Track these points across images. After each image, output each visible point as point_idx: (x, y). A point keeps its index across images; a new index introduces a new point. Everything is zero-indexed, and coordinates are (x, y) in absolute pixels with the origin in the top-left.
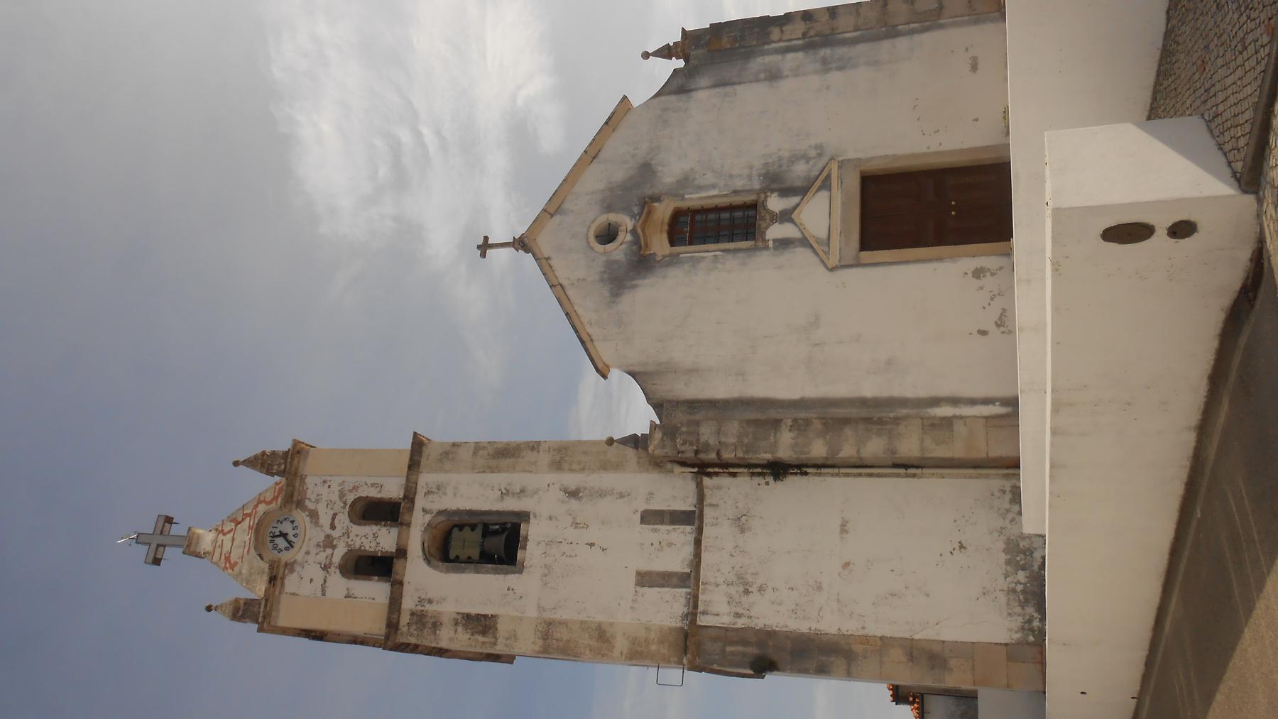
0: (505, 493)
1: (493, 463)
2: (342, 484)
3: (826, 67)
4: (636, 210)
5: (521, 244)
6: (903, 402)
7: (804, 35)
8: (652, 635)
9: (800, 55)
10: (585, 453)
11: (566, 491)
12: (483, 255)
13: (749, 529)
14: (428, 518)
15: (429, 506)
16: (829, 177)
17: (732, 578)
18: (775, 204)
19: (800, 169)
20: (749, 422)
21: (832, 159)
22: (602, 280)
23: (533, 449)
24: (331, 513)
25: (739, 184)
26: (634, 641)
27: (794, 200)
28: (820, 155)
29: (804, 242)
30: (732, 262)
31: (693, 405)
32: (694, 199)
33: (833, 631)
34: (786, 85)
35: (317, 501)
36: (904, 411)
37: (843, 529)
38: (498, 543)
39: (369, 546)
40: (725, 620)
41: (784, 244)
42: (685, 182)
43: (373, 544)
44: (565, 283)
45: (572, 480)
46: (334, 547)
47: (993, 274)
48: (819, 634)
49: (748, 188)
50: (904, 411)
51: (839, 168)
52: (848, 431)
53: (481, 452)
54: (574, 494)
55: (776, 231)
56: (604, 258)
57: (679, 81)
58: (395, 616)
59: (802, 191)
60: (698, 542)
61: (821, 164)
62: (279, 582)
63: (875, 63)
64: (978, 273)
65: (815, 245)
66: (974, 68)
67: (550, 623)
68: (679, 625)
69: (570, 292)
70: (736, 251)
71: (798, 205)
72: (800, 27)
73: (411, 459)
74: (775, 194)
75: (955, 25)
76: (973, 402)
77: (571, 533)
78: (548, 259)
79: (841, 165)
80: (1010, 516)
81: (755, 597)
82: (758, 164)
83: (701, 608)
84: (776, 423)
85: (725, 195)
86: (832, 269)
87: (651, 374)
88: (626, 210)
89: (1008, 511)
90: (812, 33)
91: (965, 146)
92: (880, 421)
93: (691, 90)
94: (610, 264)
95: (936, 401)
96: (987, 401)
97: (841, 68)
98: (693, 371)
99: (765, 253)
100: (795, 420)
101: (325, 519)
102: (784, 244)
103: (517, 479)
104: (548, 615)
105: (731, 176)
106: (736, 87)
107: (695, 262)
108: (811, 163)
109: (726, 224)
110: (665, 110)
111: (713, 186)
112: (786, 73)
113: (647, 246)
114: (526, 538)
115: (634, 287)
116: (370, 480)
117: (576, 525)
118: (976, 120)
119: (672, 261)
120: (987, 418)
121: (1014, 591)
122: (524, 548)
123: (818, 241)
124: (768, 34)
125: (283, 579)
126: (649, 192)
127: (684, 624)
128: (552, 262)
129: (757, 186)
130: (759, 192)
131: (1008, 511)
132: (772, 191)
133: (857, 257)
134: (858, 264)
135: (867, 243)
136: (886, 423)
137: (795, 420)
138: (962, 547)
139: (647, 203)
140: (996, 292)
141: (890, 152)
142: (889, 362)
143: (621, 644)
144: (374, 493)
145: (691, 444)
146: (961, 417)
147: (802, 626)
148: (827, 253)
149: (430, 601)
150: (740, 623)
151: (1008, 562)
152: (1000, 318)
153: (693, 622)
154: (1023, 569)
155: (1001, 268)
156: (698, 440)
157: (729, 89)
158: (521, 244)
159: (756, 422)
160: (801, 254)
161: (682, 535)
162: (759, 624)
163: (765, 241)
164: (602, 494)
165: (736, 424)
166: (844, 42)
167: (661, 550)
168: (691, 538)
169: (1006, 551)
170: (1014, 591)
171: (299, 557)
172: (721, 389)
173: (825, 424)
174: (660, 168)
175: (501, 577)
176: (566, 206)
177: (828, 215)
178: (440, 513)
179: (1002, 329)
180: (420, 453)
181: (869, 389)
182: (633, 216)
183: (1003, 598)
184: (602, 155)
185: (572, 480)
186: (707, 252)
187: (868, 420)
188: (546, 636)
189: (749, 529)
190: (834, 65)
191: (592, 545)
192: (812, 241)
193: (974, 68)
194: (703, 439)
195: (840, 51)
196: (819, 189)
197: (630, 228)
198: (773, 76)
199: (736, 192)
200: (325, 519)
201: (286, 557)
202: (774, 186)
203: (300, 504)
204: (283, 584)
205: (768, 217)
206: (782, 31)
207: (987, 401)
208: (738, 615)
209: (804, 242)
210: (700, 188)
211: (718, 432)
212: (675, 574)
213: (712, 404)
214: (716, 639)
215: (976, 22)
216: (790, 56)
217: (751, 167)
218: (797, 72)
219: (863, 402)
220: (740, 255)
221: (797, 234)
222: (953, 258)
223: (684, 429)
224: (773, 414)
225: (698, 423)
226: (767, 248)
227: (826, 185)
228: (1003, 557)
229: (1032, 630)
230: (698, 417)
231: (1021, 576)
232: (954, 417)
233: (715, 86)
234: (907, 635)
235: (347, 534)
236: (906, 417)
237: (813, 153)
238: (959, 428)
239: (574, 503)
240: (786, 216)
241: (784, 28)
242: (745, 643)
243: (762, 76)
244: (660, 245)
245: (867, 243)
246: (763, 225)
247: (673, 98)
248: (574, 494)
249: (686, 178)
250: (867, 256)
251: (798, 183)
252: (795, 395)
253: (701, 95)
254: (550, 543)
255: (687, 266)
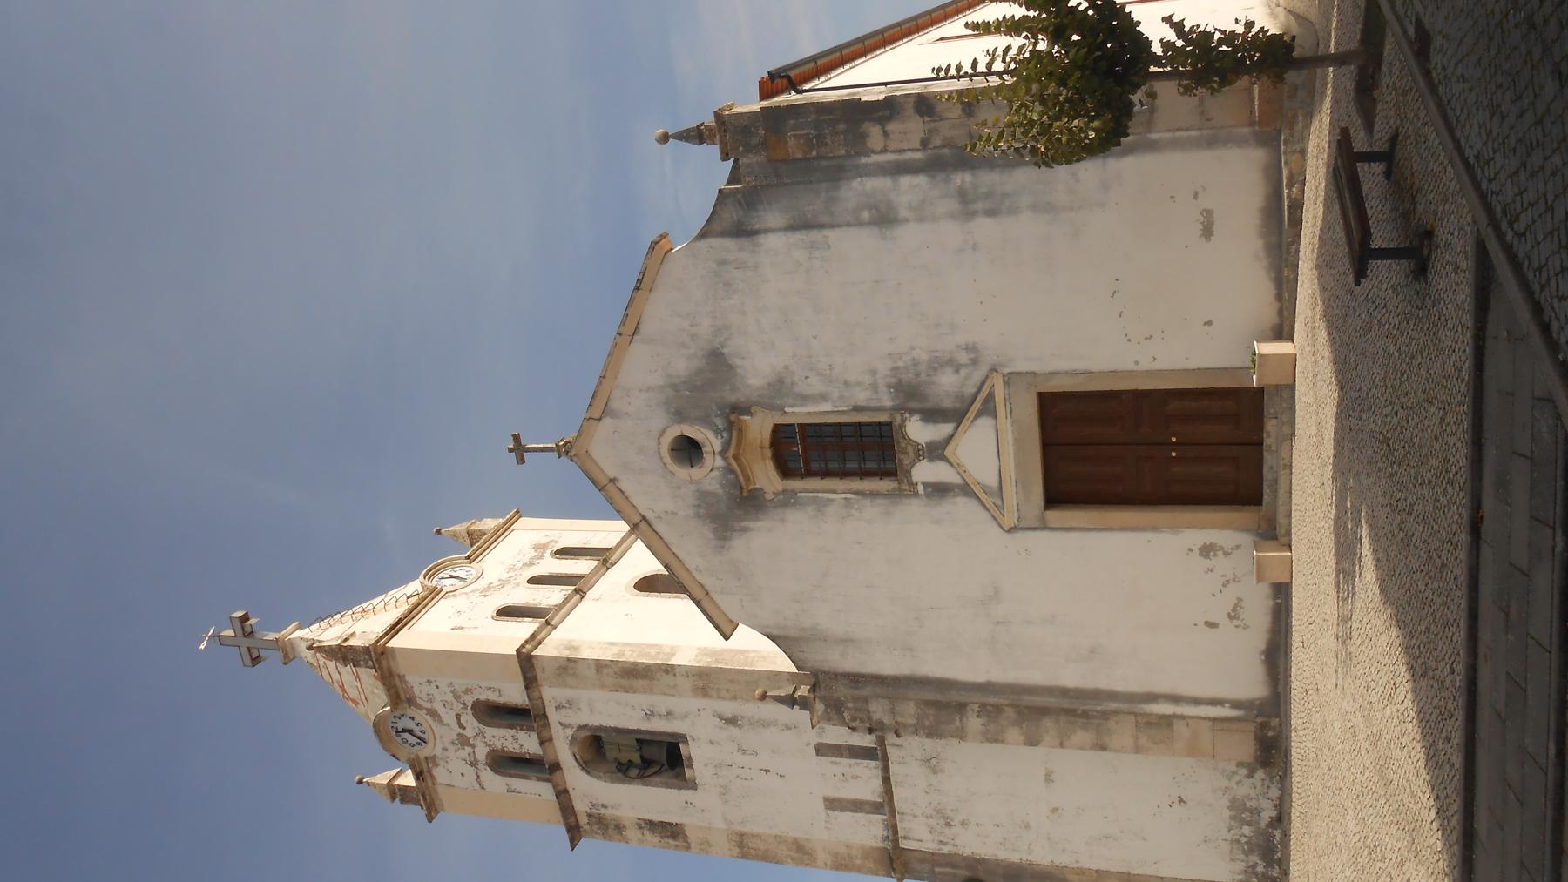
0: (650, 715)
1: (625, 682)
2: (451, 684)
3: (967, 208)
4: (720, 423)
5: (565, 450)
6: (1113, 696)
7: (924, 144)
8: (854, 852)
9: (921, 180)
10: (732, 681)
11: (721, 718)
12: (521, 460)
13: (942, 771)
14: (570, 732)
15: (563, 721)
16: (990, 397)
17: (929, 812)
18: (918, 431)
19: (947, 384)
20: (928, 703)
21: (993, 370)
22: (698, 516)
23: (667, 672)
24: (453, 714)
25: (862, 397)
26: (836, 855)
27: (945, 429)
28: (974, 362)
29: (966, 490)
30: (871, 510)
31: (856, 679)
32: (799, 413)
33: (1046, 862)
34: (909, 235)
35: (431, 701)
36: (1113, 706)
37: (1048, 778)
38: (662, 755)
39: (512, 747)
40: (929, 845)
41: (939, 490)
42: (780, 387)
43: (516, 746)
44: (649, 515)
45: (729, 708)
46: (473, 746)
47: (1226, 554)
48: (1030, 864)
49: (873, 404)
50: (1113, 706)
51: (1006, 384)
52: (1048, 722)
53: (605, 671)
54: (732, 721)
55: (924, 472)
56: (693, 488)
57: (731, 215)
58: (572, 820)
59: (956, 415)
60: (886, 780)
61: (978, 376)
62: (426, 775)
63: (1045, 208)
64: (1207, 551)
65: (983, 496)
66: (1207, 232)
67: (742, 835)
68: (881, 845)
69: (659, 528)
70: (874, 495)
71: (951, 437)
72: (911, 129)
73: (525, 678)
74: (916, 417)
75: (1176, 145)
76: (1197, 701)
77: (740, 759)
78: (612, 481)
79: (1009, 380)
80: (1237, 778)
81: (957, 829)
82: (884, 368)
83: (901, 833)
84: (961, 707)
85: (842, 412)
86: (1011, 530)
87: (796, 640)
88: (705, 421)
89: (1234, 773)
90: (937, 141)
91: (1192, 364)
92: (1085, 715)
93: (756, 233)
94: (703, 496)
95: (1153, 698)
96: (1214, 702)
97: (992, 213)
98: (847, 641)
99: (915, 501)
100: (983, 706)
101: (449, 718)
102: (939, 490)
103: (662, 703)
104: (738, 828)
105: (846, 383)
106: (827, 232)
107: (822, 505)
108: (963, 372)
109: (851, 452)
110: (722, 263)
111: (824, 397)
112: (903, 213)
113: (748, 479)
114: (690, 758)
115: (745, 530)
116: (484, 684)
117: (744, 752)
118: (1209, 323)
119: (788, 500)
120: (1214, 720)
121: (1238, 842)
122: (691, 767)
123: (985, 489)
124: (863, 137)
125: (430, 771)
126: (732, 398)
127: (888, 845)
128: (623, 486)
129: (888, 403)
130: (895, 409)
131: (1234, 773)
132: (912, 412)
133: (1043, 519)
134: (1044, 527)
135: (1054, 499)
136: (1093, 717)
137: (983, 706)
138: (1181, 800)
139: (733, 416)
140: (1230, 577)
141: (1080, 365)
142: (1092, 651)
143: (822, 857)
144: (493, 697)
145: (862, 721)
146: (1183, 717)
147: (1014, 857)
148: (1000, 508)
149: (603, 806)
150: (946, 850)
151: (1233, 818)
152: (1234, 610)
153: (896, 841)
154: (1249, 824)
155: (1238, 547)
156: (870, 718)
157: (815, 235)
158: (565, 450)
159: (935, 704)
160: (962, 506)
161: (868, 772)
162: (967, 852)
163: (912, 485)
164: (764, 724)
165: (912, 704)
166: (988, 163)
167: (846, 780)
168: (879, 773)
169: (1230, 808)
170: (1238, 842)
171: (438, 751)
172: (888, 665)
173: (1019, 713)
174: (737, 361)
175: (674, 791)
176: (616, 404)
177: (995, 451)
178: (581, 728)
179: (1236, 622)
180: (532, 667)
181: (1070, 678)
182: (717, 432)
183: (1226, 847)
184: (644, 328)
185: (729, 708)
186: (836, 491)
187: (1071, 712)
188: (741, 845)
189: (942, 771)
190: (979, 206)
191: (767, 771)
192: (977, 489)
193: (1207, 232)
194: (875, 717)
195: (988, 179)
196: (979, 415)
197: (718, 448)
198: (885, 218)
199: (858, 409)
200: (449, 718)
201: (424, 752)
202: (913, 405)
203: (411, 701)
204: (432, 777)
205: (910, 449)
206: (886, 134)
207: (1214, 702)
208: (941, 842)
209: (966, 490)
210: (805, 399)
211: (893, 712)
212: (867, 802)
213: (879, 680)
214: (923, 861)
215: (1211, 143)
216: (906, 181)
217: (874, 373)
218: (921, 214)
219: (1064, 692)
220: (880, 501)
221: (957, 480)
222: (1174, 528)
223: (850, 705)
224: (955, 697)
225: (866, 700)
226: (916, 494)
227: (988, 409)
228: (1227, 813)
229: (1256, 874)
230: (865, 692)
231: (1246, 830)
232: (1175, 716)
233: (792, 228)
234: (1124, 870)
235: (481, 734)
236: (1116, 712)
237: (963, 358)
238: (1179, 726)
239: (733, 729)
240: (935, 451)
241: (890, 127)
242: (953, 866)
243: (866, 215)
244: (766, 477)
245: (1054, 499)
246: (906, 462)
247: (729, 243)
248: (732, 721)
249: (781, 381)
250: (1054, 516)
251: (947, 403)
252: (981, 678)
253: (773, 241)
254: (719, 765)
255: (810, 509)
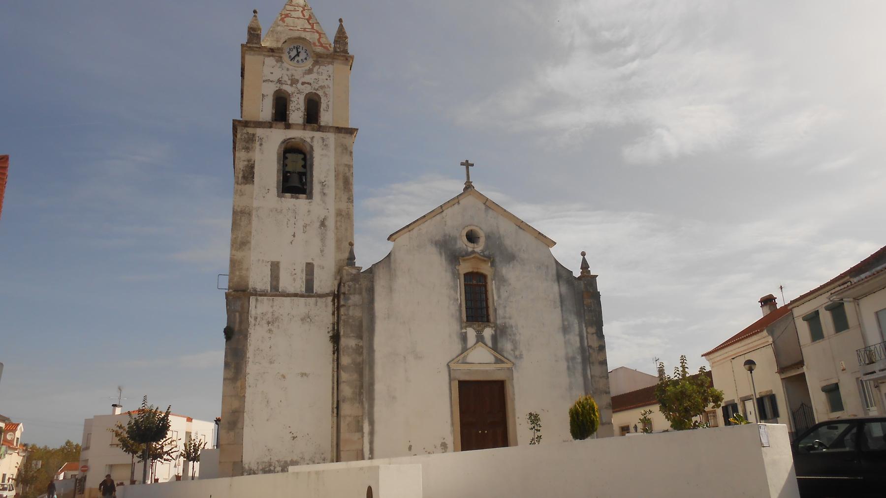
0: (323, 184)
1: (341, 176)
2: (329, 87)
3: (570, 359)
4: (486, 253)
6: (371, 406)
7: (590, 347)
8: (244, 272)
9: (578, 344)
10: (346, 230)
12: (462, 164)
14: (309, 140)
15: (315, 140)
16: (503, 362)
17: (276, 315)
18: (488, 333)
19: (507, 346)
21: (514, 364)
22: (445, 236)
23: (349, 199)
24: (311, 82)
25: (500, 312)
27: (490, 344)
28: (516, 357)
29: (465, 349)
30: (454, 309)
31: (371, 291)
32: (492, 286)
33: (248, 370)
34: (560, 337)
35: (318, 73)
36: (366, 406)
37: (303, 375)
39: (292, 106)
40: (253, 312)
41: (464, 338)
42: (502, 281)
44: (444, 214)
45: (331, 223)
46: (291, 85)
50: (366, 406)
51: (508, 369)
52: (355, 376)
53: (347, 169)
54: (323, 224)
55: (471, 333)
56: (458, 235)
59: (495, 348)
60: (296, 295)
65: (462, 356)
67: (250, 214)
69: (438, 217)
70: (460, 311)
76: (371, 443)
77: (300, 224)
78: (458, 203)
79: (510, 370)
81: (266, 327)
82: (512, 322)
83: (260, 298)
84: (360, 337)
86: (448, 365)
87: (389, 267)
88: (487, 247)
90: (591, 351)
92: (361, 394)
94: (455, 239)
95: (372, 423)
97: (568, 368)
98: (391, 290)
99: (459, 328)
101: (308, 78)
102: (464, 338)
103: (331, 191)
104: (254, 213)
105: (505, 307)
109: (477, 306)
110: (547, 267)
111: (499, 297)
112: (567, 337)
113: (464, 260)
114: (297, 198)
115: (441, 254)
116: (330, 104)
117: (305, 226)
119: (455, 275)
121: (270, 465)
122: (292, 197)
123: (465, 357)
125: (273, 56)
126: (497, 259)
128: (456, 206)
129: (498, 322)
132: (495, 331)
133: (455, 379)
134: (451, 380)
135: (463, 384)
137: (362, 347)
138: (294, 438)
139: (489, 258)
141: (517, 397)
142: (394, 398)
143: (239, 255)
144: (323, 106)
145: (349, 290)
146: (363, 437)
147: (250, 354)
149: (261, 145)
150: (251, 320)
153: (252, 294)
157: (558, 304)
159: (361, 326)
160: (457, 347)
161: (299, 286)
162: (251, 330)
164: (323, 240)
165: (360, 315)
166: (584, 370)
167: (292, 275)
168: (298, 291)
170: (270, 465)
171: (285, 65)
172: (380, 305)
175: (275, 185)
176: (491, 213)
177: (481, 361)
178: (312, 147)
181: (379, 387)
182: (483, 251)
183: (266, 459)
184: (521, 231)
185: (331, 223)
186: (460, 295)
188: (242, 212)
190: (571, 364)
191: (294, 236)
192: (465, 354)
194: (352, 297)
195: (579, 367)
197: (476, 250)
198: (565, 330)
199: (495, 310)
200: (308, 78)
201: (285, 57)
202: (498, 332)
203: (316, 63)
204: (269, 56)
208: (256, 319)
209: (465, 349)
210: (498, 289)
211: (355, 305)
213: (371, 301)
216: (578, 339)
217: (510, 318)
218: (567, 343)
219: (372, 384)
220: (458, 313)
222: (454, 431)
224: (365, 335)
225: (360, 293)
226: (462, 328)
227: (498, 361)
230: (364, 293)
232: (363, 433)
233: (561, 295)
234: (246, 409)
235: (299, 92)
236: (363, 408)
237: (517, 353)
238: (358, 435)
240: (480, 338)
242: (241, 322)
243: (566, 323)
244: (465, 267)
245: (463, 384)
247: (554, 272)
248: (323, 224)
251: (500, 345)
252: (377, 346)
253: (556, 287)
254: (295, 212)
